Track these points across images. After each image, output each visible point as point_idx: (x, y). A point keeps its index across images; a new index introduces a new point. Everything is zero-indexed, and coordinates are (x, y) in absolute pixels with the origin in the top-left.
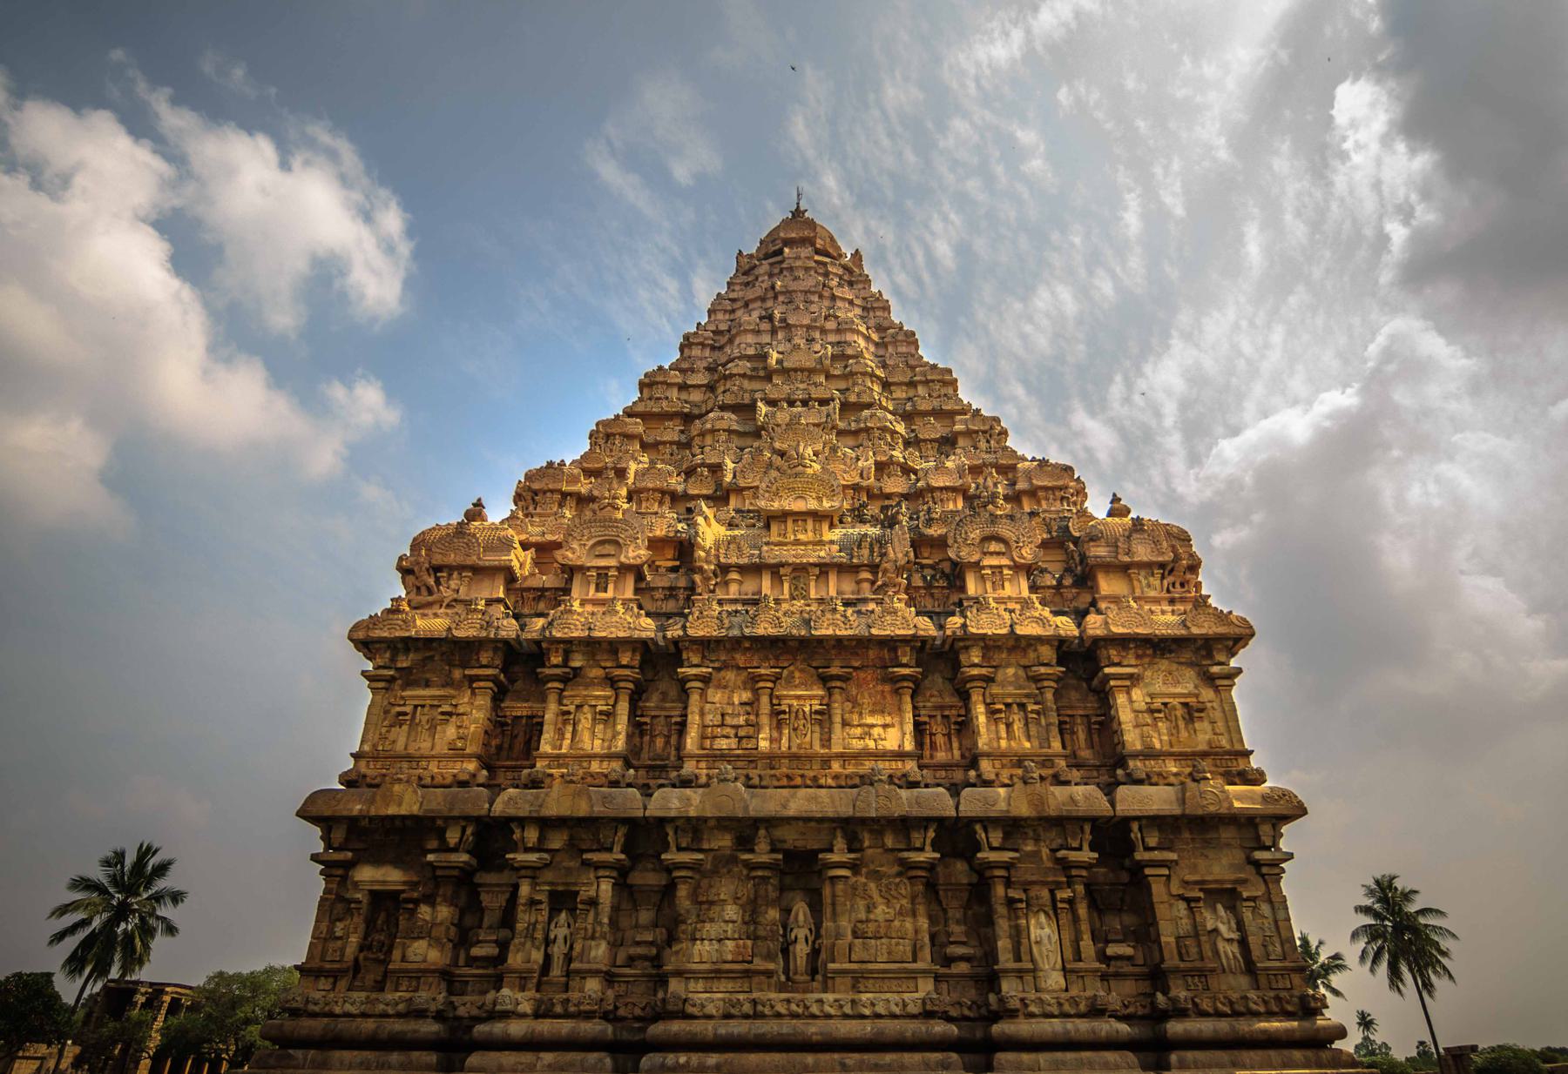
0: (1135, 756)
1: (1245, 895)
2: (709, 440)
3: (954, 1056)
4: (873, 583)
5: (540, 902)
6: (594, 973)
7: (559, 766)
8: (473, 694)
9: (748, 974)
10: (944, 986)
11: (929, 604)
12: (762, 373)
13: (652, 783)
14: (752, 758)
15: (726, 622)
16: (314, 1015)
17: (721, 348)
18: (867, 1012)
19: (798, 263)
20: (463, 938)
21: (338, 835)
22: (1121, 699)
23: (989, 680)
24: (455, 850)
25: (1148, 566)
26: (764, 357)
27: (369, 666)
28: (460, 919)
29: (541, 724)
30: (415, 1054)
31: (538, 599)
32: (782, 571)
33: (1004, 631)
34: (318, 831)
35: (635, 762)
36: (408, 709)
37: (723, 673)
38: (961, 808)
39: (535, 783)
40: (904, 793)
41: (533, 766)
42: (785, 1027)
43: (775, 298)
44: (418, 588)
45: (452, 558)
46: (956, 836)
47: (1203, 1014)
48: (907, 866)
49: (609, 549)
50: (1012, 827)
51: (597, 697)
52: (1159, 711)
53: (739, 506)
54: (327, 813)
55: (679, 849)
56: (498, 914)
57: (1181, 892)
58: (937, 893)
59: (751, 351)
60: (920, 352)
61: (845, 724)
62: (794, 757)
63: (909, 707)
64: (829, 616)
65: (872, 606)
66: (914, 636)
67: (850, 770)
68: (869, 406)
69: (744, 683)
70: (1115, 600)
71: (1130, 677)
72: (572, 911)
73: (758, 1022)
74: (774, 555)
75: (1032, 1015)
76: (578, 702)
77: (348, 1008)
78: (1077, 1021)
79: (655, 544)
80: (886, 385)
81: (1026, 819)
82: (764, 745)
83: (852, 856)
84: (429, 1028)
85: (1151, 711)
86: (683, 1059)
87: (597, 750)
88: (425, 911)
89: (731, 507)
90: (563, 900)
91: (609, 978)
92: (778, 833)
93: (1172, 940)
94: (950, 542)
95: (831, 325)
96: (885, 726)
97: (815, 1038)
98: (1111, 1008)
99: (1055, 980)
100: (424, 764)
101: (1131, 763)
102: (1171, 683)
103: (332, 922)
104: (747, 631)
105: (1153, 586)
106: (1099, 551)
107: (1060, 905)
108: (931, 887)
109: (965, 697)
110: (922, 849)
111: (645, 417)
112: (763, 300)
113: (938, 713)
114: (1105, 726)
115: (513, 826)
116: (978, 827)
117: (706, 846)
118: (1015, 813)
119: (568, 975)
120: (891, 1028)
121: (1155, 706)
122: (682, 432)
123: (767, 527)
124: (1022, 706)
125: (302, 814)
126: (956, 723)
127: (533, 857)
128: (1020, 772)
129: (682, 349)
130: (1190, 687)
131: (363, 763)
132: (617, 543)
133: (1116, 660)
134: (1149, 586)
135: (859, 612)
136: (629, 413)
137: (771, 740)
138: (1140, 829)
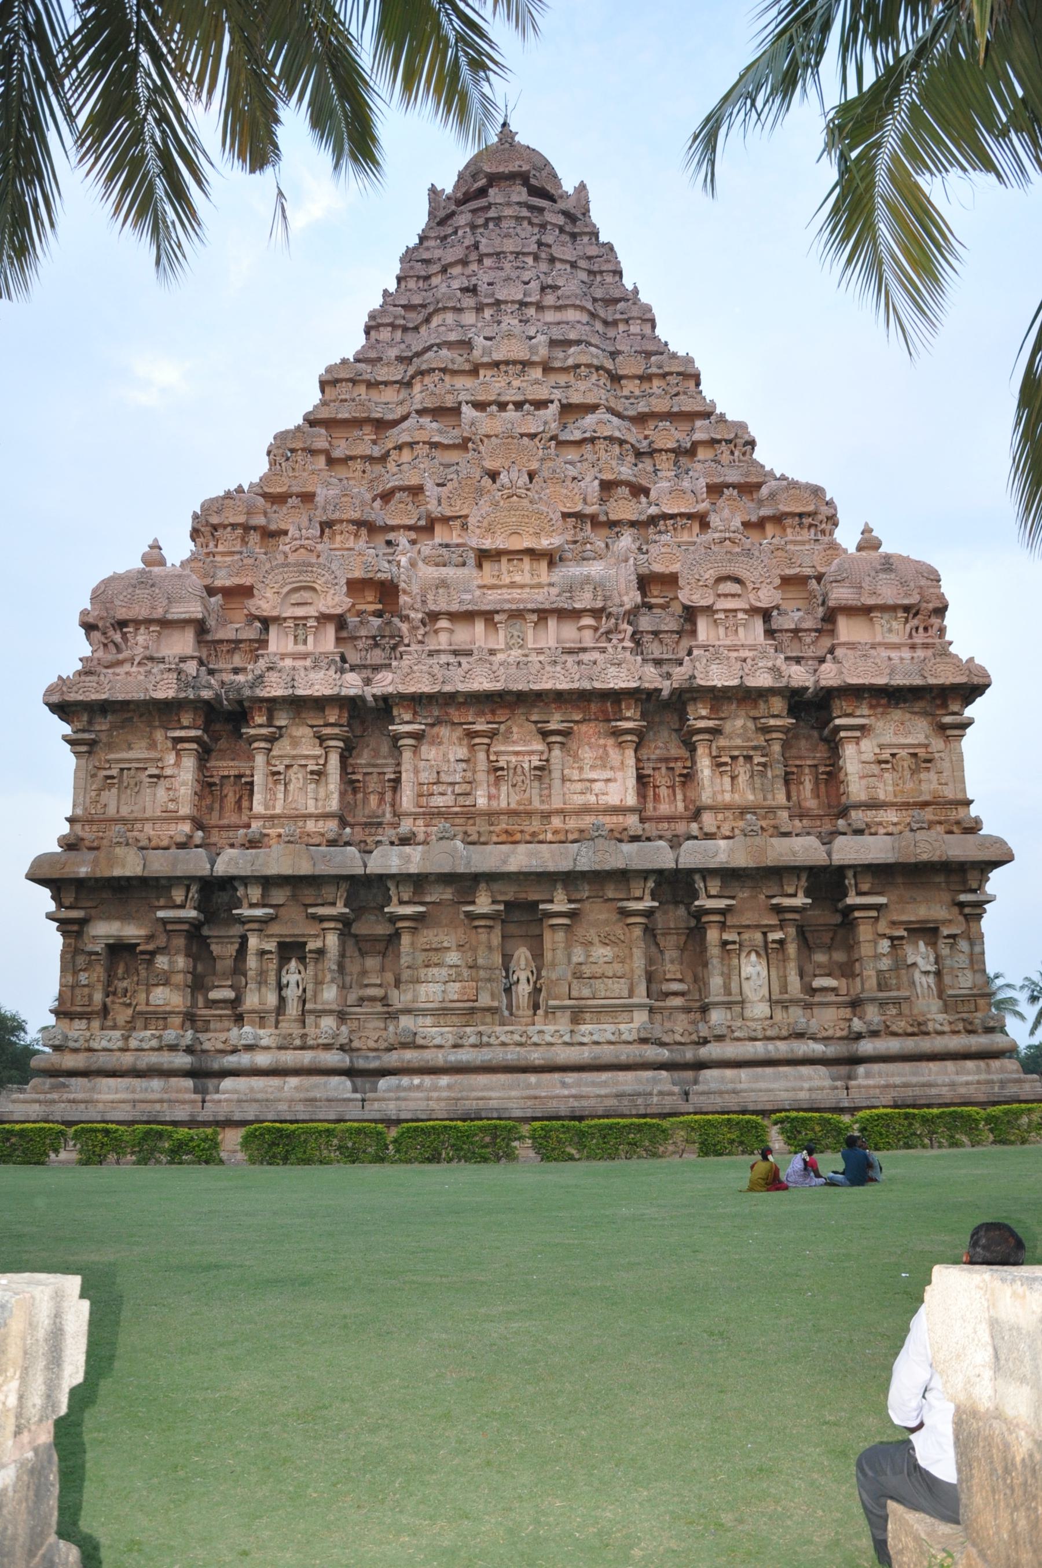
0: (857, 806)
1: (945, 932)
2: (406, 455)
3: (664, 1073)
4: (596, 629)
5: (270, 952)
6: (330, 1012)
7: (273, 827)
8: (178, 755)
9: (472, 1011)
10: (658, 1017)
11: (655, 650)
12: (467, 367)
13: (369, 840)
14: (470, 815)
15: (439, 676)
16: (76, 1050)
17: (416, 329)
18: (585, 1040)
19: (508, 212)
20: (198, 985)
22: (849, 751)
23: (716, 732)
24: (182, 906)
25: (893, 608)
26: (467, 345)
27: (67, 729)
28: (195, 967)
29: (251, 783)
30: (174, 1081)
31: (231, 652)
32: (497, 618)
33: (735, 682)
34: (46, 893)
35: (349, 819)
36: (114, 772)
37: (436, 729)
38: (681, 860)
39: (253, 843)
40: (627, 848)
41: (248, 826)
42: (512, 1055)
43: (480, 261)
44: (105, 645)
45: (143, 613)
46: (676, 885)
47: (894, 1034)
48: (624, 913)
49: (306, 595)
50: (730, 876)
51: (307, 757)
52: (887, 762)
53: (446, 540)
54: (56, 875)
55: (401, 902)
56: (229, 963)
57: (888, 931)
58: (655, 936)
59: (453, 337)
60: (658, 332)
61: (564, 780)
62: (512, 813)
63: (631, 762)
64: (548, 668)
65: (596, 655)
66: (637, 690)
67: (572, 823)
68: (593, 408)
69: (460, 739)
70: (852, 646)
71: (862, 728)
72: (302, 959)
73: (485, 1050)
74: (491, 600)
75: (738, 1039)
76: (287, 762)
77: (104, 1044)
78: (779, 1043)
79: (355, 586)
80: (616, 378)
81: (745, 869)
82: (482, 802)
83: (573, 906)
84: (183, 1060)
85: (880, 762)
86: (417, 1080)
87: (311, 809)
88: (162, 962)
89: (438, 540)
90: (291, 950)
91: (342, 1016)
93: (873, 973)
94: (681, 582)
95: (550, 299)
96: (608, 780)
97: (537, 1062)
98: (811, 1031)
99: (759, 1010)
100: (138, 826)
101: (853, 813)
102: (903, 731)
103: (76, 973)
104: (461, 687)
105: (893, 630)
106: (840, 595)
107: (771, 946)
108: (650, 931)
109: (692, 749)
110: (640, 899)
111: (329, 424)
112: (464, 262)
113: (663, 766)
114: (831, 776)
115: (236, 884)
116: (697, 877)
117: (428, 899)
118: (733, 864)
119: (303, 1015)
120: (607, 1054)
121: (883, 757)
122: (374, 442)
123: (480, 566)
124: (748, 758)
125: (36, 877)
126: (681, 775)
127: (259, 912)
128: (741, 824)
129: (367, 332)
131: (78, 827)
132: (314, 589)
133: (849, 711)
134: (890, 630)
135: (579, 663)
136: (311, 421)
137: (490, 797)
138: (855, 876)
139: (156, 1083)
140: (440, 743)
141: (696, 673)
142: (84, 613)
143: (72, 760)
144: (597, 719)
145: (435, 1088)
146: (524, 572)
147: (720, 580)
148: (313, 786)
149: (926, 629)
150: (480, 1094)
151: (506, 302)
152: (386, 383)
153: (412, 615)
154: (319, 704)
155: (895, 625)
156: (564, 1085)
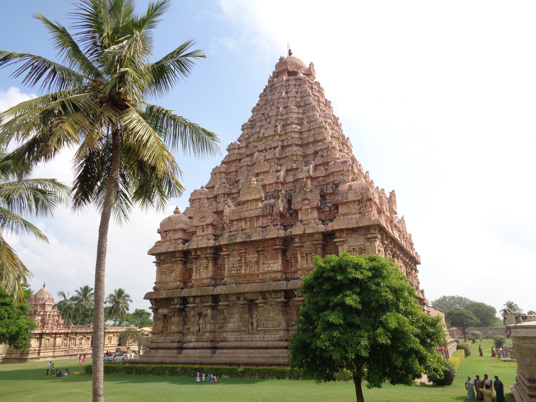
18: (266, 340)
21: (154, 303)
23: (302, 247)
24: (176, 304)
32: (247, 220)
41: (191, 282)
49: (204, 219)
61: (264, 264)
62: (250, 275)
71: (343, 241)
77: (161, 341)
82: (243, 272)
84: (175, 345)
86: (225, 351)
92: (246, 295)
113: (293, 256)
120: (271, 344)
130: (362, 242)
134: (354, 208)
139: (169, 351)
142: (158, 230)
143: (155, 268)
145: (229, 353)
149: (365, 206)
150: (237, 355)
154: (206, 248)
155: (355, 206)
156: (259, 353)
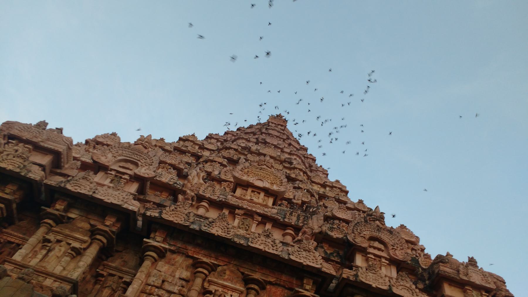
32: (237, 211)
33: (385, 288)
37: (174, 256)
49: (131, 166)
64: (263, 238)
76: (59, 238)
104: (204, 228)
140: (173, 265)
141: (359, 274)
144: (284, 287)
146: (260, 198)
147: (372, 239)
148: (68, 259)
151: (269, 143)
152: (207, 149)
153: (188, 192)
